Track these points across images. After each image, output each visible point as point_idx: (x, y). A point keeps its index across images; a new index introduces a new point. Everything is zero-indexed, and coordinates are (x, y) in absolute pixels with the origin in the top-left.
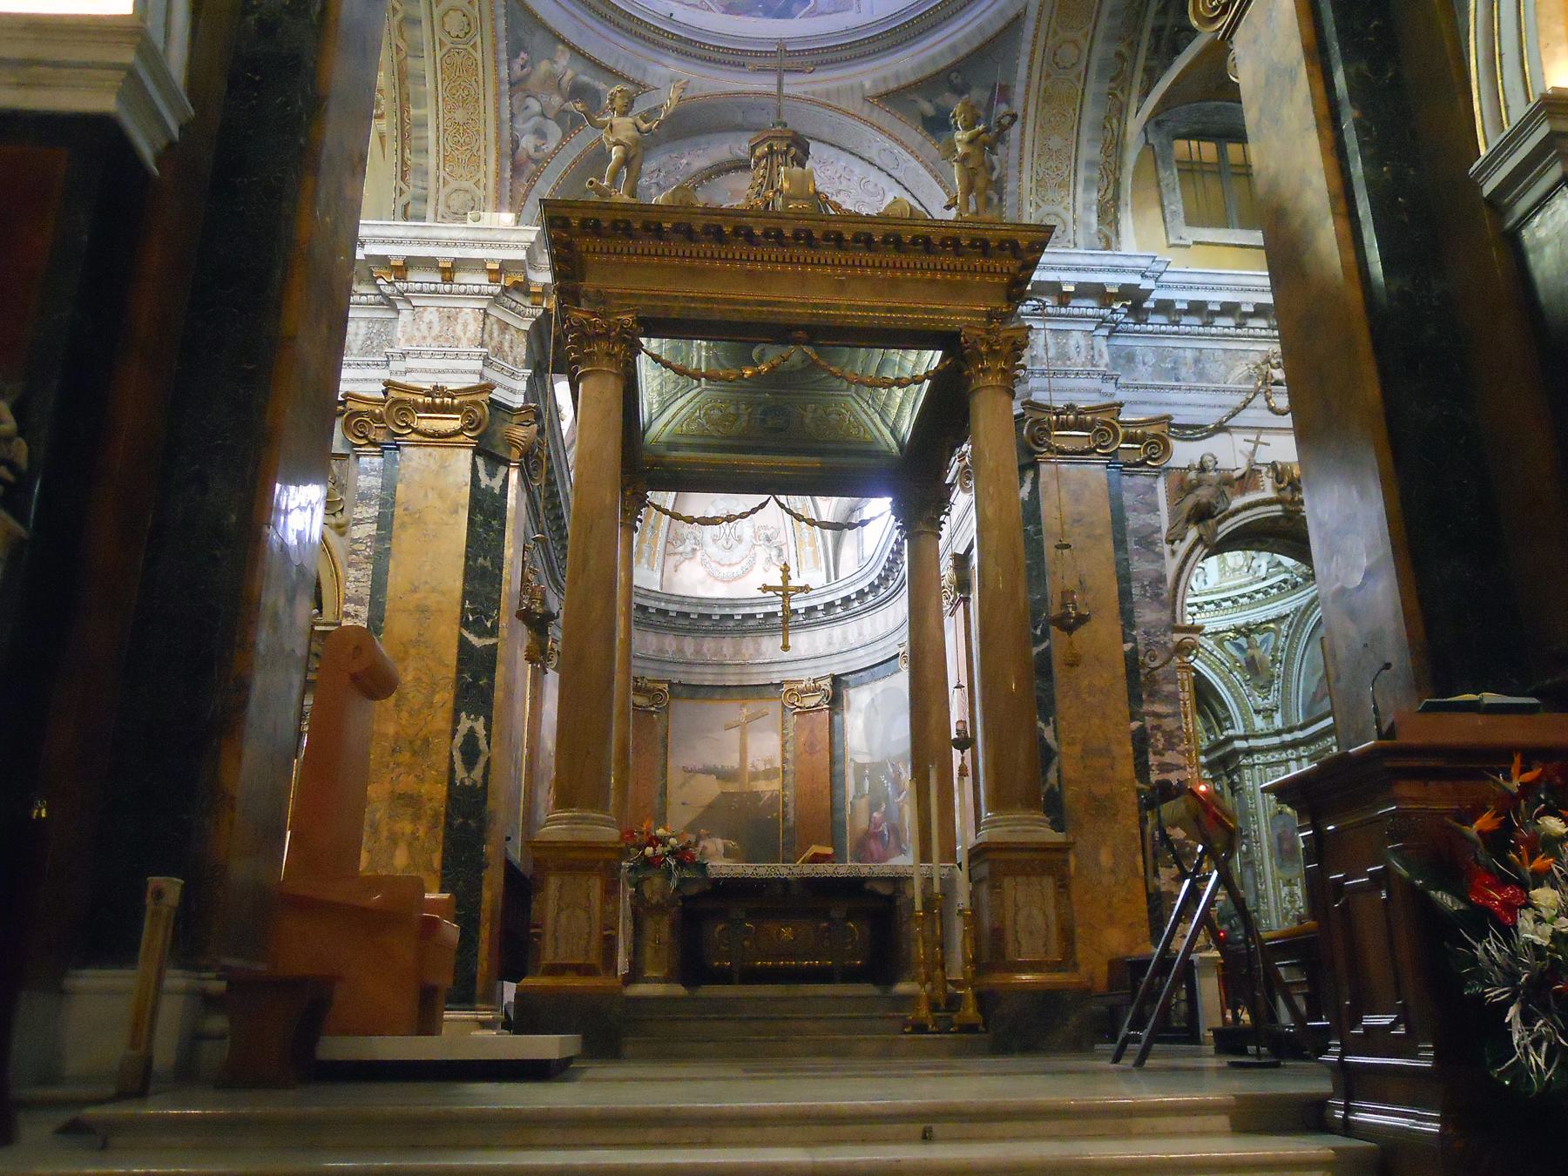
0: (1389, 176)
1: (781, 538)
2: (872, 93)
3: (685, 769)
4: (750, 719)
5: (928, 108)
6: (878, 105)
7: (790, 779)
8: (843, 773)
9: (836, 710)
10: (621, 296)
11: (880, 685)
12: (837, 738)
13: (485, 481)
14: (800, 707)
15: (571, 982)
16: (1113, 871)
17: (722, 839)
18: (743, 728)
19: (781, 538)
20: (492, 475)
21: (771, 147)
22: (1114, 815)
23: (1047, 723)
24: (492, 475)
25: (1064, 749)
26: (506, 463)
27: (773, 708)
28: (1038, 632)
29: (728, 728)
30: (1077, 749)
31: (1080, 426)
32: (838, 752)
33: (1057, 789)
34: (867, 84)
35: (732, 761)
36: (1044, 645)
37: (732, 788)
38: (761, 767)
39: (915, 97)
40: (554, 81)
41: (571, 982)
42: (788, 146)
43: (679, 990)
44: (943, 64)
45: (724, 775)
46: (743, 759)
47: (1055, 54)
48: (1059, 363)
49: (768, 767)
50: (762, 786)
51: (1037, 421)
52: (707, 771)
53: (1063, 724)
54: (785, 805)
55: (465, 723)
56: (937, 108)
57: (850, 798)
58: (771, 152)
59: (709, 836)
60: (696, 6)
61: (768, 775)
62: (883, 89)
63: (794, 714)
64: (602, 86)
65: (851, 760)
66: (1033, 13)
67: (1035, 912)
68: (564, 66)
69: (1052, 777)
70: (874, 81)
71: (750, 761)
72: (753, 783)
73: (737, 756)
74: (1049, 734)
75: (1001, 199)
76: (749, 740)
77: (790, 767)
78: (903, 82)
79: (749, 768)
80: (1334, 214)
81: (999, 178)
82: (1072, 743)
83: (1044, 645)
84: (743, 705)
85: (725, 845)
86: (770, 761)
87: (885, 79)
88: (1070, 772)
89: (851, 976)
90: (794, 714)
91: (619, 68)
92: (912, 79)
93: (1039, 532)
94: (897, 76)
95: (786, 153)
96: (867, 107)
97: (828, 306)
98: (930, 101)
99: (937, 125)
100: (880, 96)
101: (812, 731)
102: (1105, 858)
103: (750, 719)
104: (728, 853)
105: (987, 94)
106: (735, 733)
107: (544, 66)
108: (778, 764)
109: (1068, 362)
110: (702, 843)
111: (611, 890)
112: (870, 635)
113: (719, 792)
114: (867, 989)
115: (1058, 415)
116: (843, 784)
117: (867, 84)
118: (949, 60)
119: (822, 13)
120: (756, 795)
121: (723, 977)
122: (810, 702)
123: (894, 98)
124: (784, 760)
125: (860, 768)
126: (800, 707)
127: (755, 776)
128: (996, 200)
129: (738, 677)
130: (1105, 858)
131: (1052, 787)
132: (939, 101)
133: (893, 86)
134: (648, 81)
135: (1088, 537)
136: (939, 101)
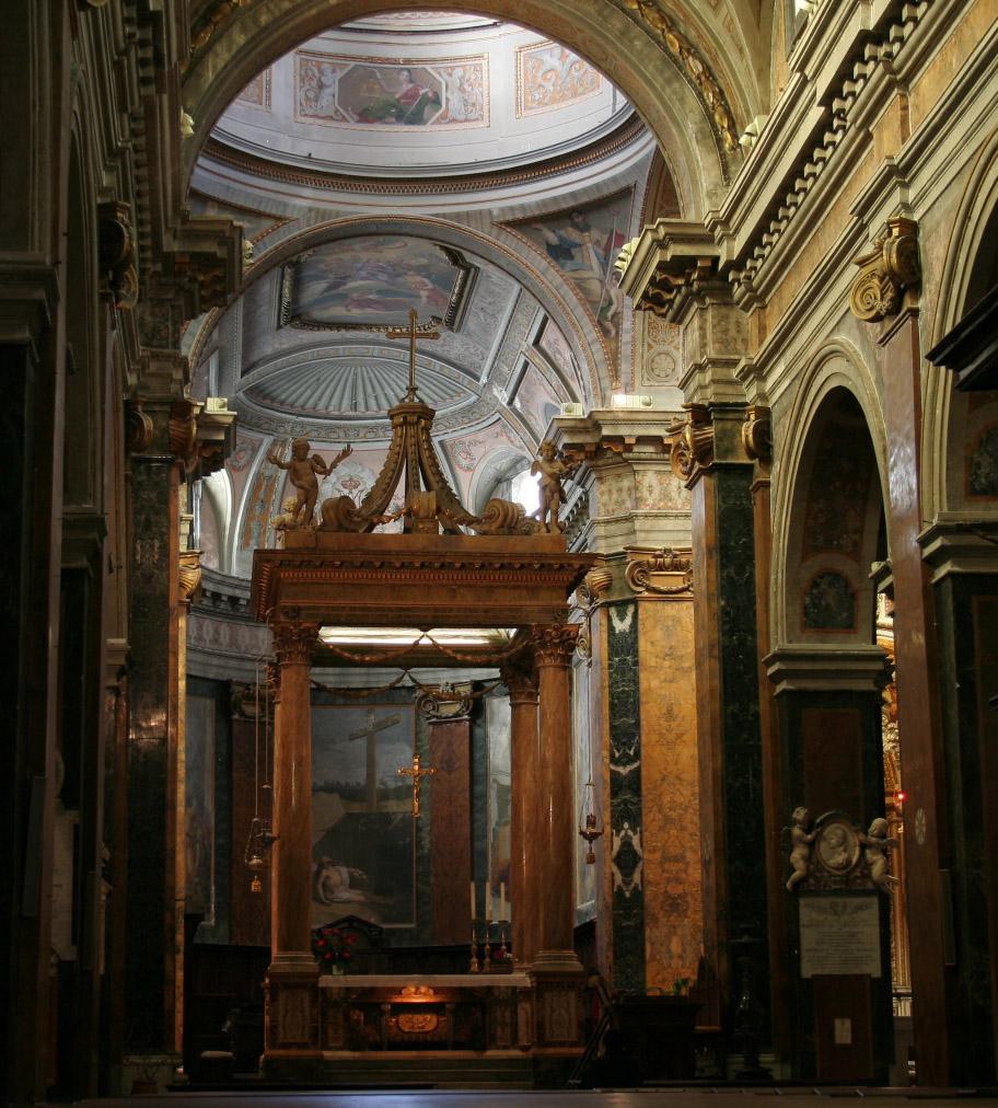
0: (736, 642)
2: (502, 219)
4: (381, 726)
5: (553, 239)
8: (485, 796)
9: (479, 722)
10: (308, 608)
12: (478, 755)
14: (437, 717)
15: (293, 1053)
16: (680, 957)
17: (348, 866)
18: (371, 737)
21: (405, 418)
22: (686, 910)
23: (635, 833)
25: (646, 856)
27: (406, 715)
28: (632, 752)
29: (353, 738)
30: (658, 855)
31: (677, 567)
32: (479, 771)
33: (640, 888)
35: (359, 776)
36: (636, 765)
37: (356, 808)
38: (392, 784)
39: (539, 226)
41: (293, 1053)
42: (419, 418)
45: (349, 794)
46: (371, 775)
48: (662, 504)
49: (400, 784)
50: (392, 806)
51: (638, 564)
52: (330, 789)
53: (646, 834)
54: (419, 830)
56: (561, 238)
57: (492, 824)
58: (405, 422)
59: (333, 864)
60: (331, 118)
61: (403, 793)
62: (509, 217)
63: (430, 724)
65: (495, 781)
67: (564, 1013)
69: (636, 877)
71: (379, 776)
72: (383, 803)
73: (363, 771)
74: (636, 841)
75: (617, 333)
76: (377, 752)
78: (529, 214)
79: (378, 785)
80: (711, 656)
81: (615, 315)
82: (654, 850)
83: (636, 765)
84: (369, 712)
85: (351, 875)
87: (512, 209)
88: (650, 876)
89: (457, 1046)
90: (430, 724)
91: (262, 209)
92: (537, 213)
93: (636, 663)
94: (523, 207)
95: (418, 423)
96: (495, 231)
97: (444, 610)
98: (554, 232)
99: (561, 253)
100: (508, 224)
101: (450, 744)
102: (675, 946)
103: (381, 726)
105: (606, 237)
106: (361, 743)
109: (670, 504)
110: (324, 873)
112: (504, 701)
113: (342, 812)
115: (656, 557)
116: (485, 809)
117: (495, 213)
118: (571, 203)
119: (454, 120)
120: (386, 818)
122: (449, 710)
123: (524, 224)
125: (501, 788)
126: (437, 717)
127: (385, 795)
128: (613, 333)
129: (364, 679)
130: (675, 946)
131: (636, 888)
133: (519, 215)
134: (288, 215)
135: (677, 669)
136: (562, 232)
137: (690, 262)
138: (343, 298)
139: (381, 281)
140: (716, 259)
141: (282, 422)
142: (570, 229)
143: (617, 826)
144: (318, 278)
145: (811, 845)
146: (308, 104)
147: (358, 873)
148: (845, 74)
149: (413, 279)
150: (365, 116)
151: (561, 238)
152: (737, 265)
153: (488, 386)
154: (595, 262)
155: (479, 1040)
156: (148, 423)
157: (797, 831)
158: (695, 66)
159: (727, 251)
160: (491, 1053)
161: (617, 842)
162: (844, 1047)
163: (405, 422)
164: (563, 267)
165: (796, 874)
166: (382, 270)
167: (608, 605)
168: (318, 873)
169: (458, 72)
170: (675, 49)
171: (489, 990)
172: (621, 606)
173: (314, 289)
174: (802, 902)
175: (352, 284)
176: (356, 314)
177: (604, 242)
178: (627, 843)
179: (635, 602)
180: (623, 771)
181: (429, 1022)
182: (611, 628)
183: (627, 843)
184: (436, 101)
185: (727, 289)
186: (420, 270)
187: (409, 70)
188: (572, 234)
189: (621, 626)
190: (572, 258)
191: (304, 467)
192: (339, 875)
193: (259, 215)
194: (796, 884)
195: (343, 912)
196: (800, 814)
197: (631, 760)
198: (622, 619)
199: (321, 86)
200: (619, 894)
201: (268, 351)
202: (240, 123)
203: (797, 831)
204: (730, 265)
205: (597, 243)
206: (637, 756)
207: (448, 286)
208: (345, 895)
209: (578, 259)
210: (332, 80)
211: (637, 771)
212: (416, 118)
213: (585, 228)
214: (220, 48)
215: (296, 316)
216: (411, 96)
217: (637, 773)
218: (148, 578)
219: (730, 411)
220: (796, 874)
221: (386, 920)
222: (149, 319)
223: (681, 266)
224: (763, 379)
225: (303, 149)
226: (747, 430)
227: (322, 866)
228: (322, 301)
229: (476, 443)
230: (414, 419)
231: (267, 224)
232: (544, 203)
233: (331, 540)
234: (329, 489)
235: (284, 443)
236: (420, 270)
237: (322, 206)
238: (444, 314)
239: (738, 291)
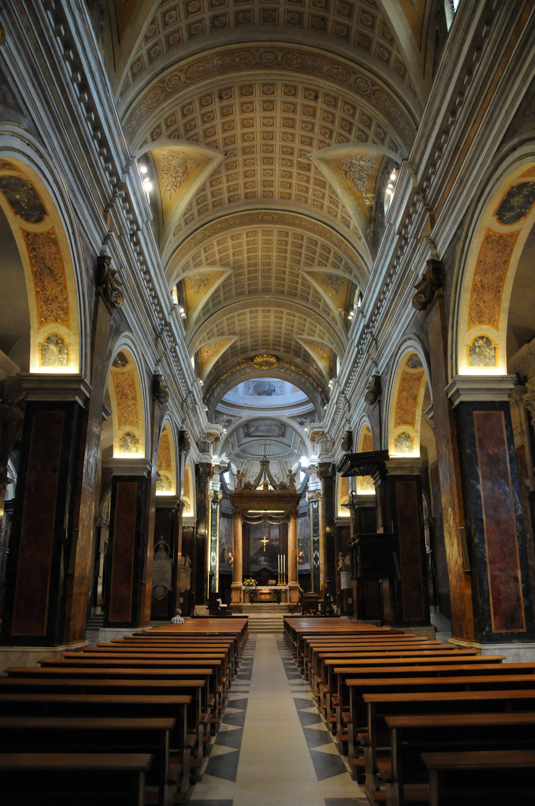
1: (278, 476)
3: (254, 539)
5: (300, 421)
7: (281, 541)
11: (303, 518)
13: (213, 507)
15: (236, 604)
19: (278, 476)
20: (214, 505)
24: (214, 505)
26: (217, 502)
38: (274, 538)
40: (223, 421)
43: (250, 604)
55: (212, 554)
61: (276, 540)
64: (232, 419)
68: (225, 418)
69: (318, 563)
77: (281, 538)
86: (276, 537)
89: (274, 602)
104: (265, 561)
106: (267, 529)
107: (221, 419)
108: (278, 537)
111: (241, 592)
114: (276, 604)
121: (256, 602)
123: (293, 418)
124: (280, 536)
137: (318, 432)
138: (259, 431)
139: (267, 427)
140: (323, 432)
141: (248, 457)
143: (314, 551)
144: (252, 427)
145: (343, 560)
146: (246, 392)
147: (266, 558)
148: (338, 398)
149: (274, 427)
150: (259, 394)
152: (328, 433)
153: (293, 449)
155: (279, 601)
156: (201, 469)
157: (340, 557)
158: (320, 390)
159: (326, 430)
160: (281, 604)
161: (314, 555)
162: (350, 604)
165: (340, 567)
166: (267, 425)
167: (312, 502)
168: (257, 558)
169: (279, 384)
170: (315, 385)
171: (281, 590)
172: (315, 502)
173: (252, 429)
174: (341, 572)
175: (260, 428)
176: (263, 434)
178: (316, 555)
179: (318, 501)
180: (316, 539)
181: (268, 597)
182: (313, 507)
183: (316, 555)
184: (274, 391)
185: (327, 438)
186: (275, 425)
188: (304, 420)
189: (315, 506)
191: (239, 475)
192: (262, 559)
193: (235, 416)
194: (340, 569)
195: (263, 567)
196: (341, 553)
197: (317, 537)
198: (315, 504)
199: (249, 388)
200: (314, 567)
201: (244, 442)
202: (229, 397)
203: (340, 557)
204: (327, 433)
206: (318, 535)
207: (282, 429)
208: (264, 563)
210: (252, 387)
211: (318, 539)
212: (270, 394)
214: (218, 388)
215: (248, 435)
216: (269, 389)
217: (318, 539)
218: (201, 502)
219: (328, 464)
220: (340, 567)
221: (273, 568)
222: (202, 446)
223: (317, 433)
224: (334, 457)
225: (246, 402)
226: (330, 469)
227: (258, 557)
228: (255, 431)
229: (291, 461)
230: (265, 464)
231: (237, 418)
232: (297, 413)
233: (245, 491)
234: (245, 481)
235: (249, 461)
236: (275, 425)
237: (249, 414)
238: (281, 434)
239: (329, 438)
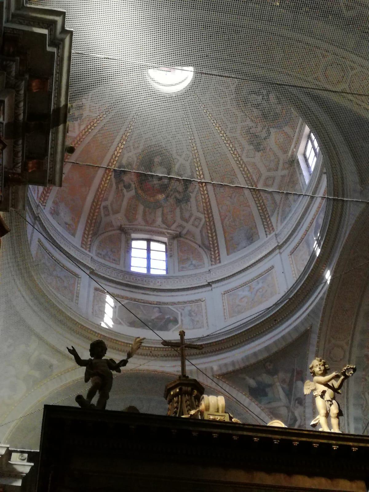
2: (219, 373)
5: (252, 383)
6: (225, 382)
21: (180, 389)
34: (215, 368)
44: (260, 358)
47: (330, 353)
56: (259, 383)
58: (181, 393)
62: (224, 371)
66: (316, 329)
70: (220, 366)
78: (237, 367)
87: (226, 365)
92: (242, 365)
94: (233, 363)
98: (254, 379)
117: (215, 368)
118: (266, 355)
132: (259, 379)
133: (231, 369)
136: (259, 379)
142: (264, 375)
151: (259, 383)
154: (282, 395)
163: (181, 393)
164: (260, 402)
177: (288, 380)
187: (159, 307)
188: (266, 378)
190: (266, 395)
205: (283, 381)
209: (270, 395)
213: (273, 373)
232: (247, 358)
